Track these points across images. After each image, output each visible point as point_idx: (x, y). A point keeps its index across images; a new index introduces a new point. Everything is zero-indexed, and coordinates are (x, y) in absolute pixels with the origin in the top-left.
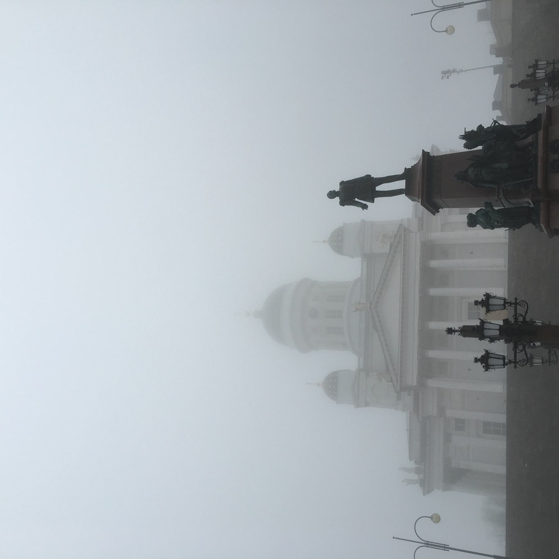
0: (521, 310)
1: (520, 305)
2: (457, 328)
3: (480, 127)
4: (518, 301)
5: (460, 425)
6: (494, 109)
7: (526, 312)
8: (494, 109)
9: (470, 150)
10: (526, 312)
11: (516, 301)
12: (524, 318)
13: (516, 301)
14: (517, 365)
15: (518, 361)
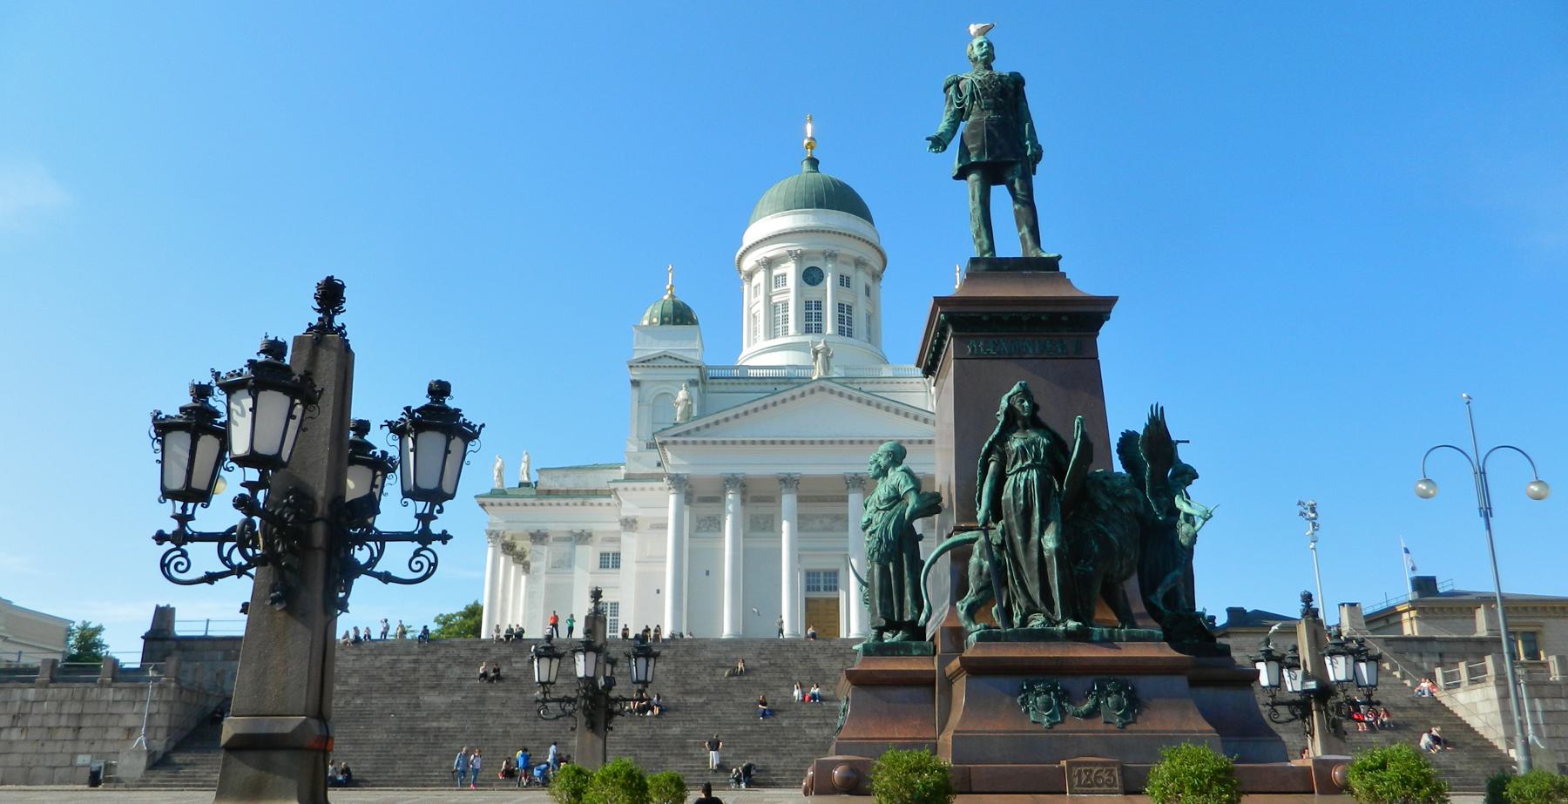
0: (396, 557)
1: (417, 553)
2: (338, 321)
3: (1189, 475)
4: (436, 545)
5: (610, 561)
6: (1231, 611)
7: (386, 578)
8: (1231, 611)
9: (1114, 448)
10: (386, 578)
11: (437, 537)
12: (368, 569)
13: (437, 537)
14: (168, 545)
15: (189, 547)
